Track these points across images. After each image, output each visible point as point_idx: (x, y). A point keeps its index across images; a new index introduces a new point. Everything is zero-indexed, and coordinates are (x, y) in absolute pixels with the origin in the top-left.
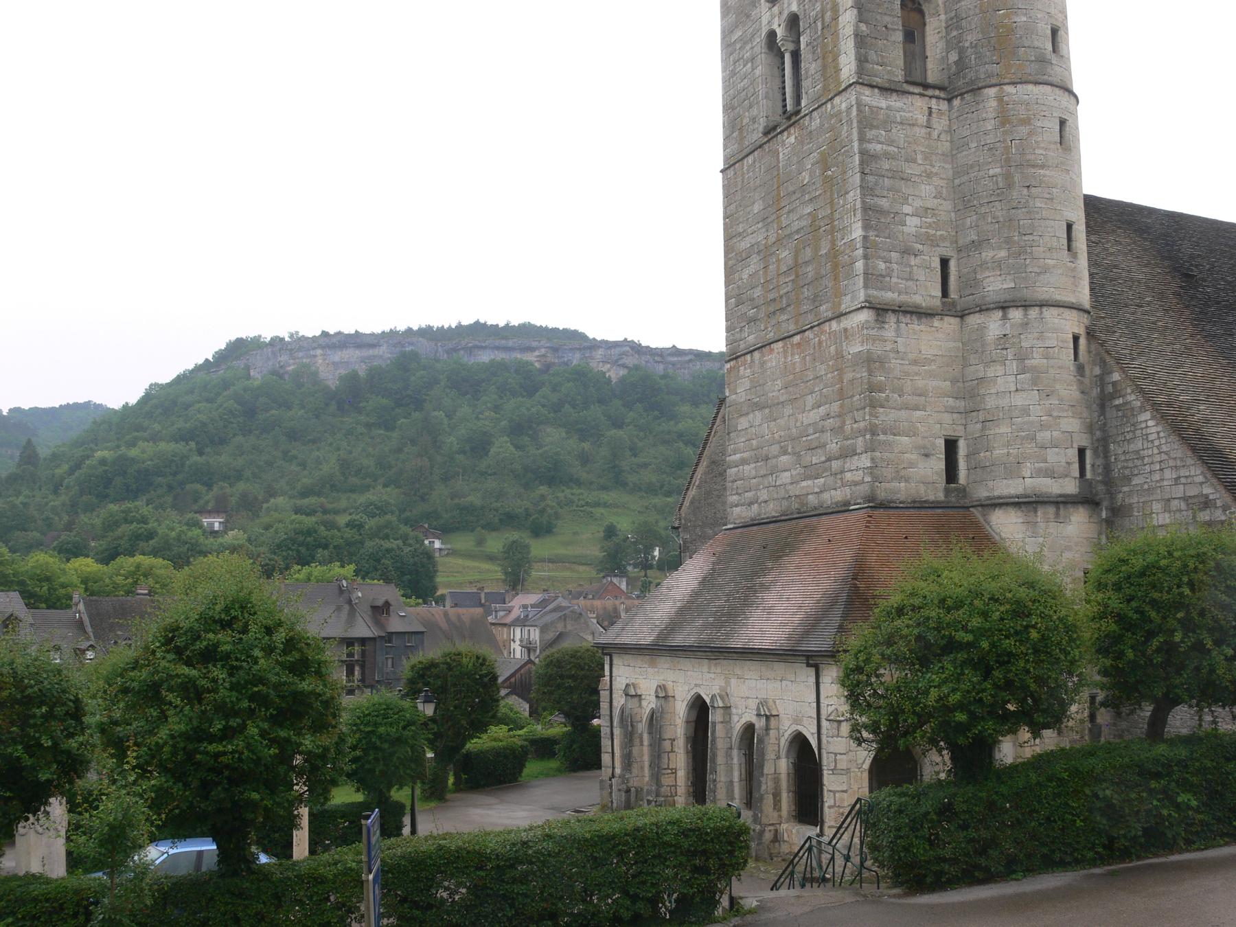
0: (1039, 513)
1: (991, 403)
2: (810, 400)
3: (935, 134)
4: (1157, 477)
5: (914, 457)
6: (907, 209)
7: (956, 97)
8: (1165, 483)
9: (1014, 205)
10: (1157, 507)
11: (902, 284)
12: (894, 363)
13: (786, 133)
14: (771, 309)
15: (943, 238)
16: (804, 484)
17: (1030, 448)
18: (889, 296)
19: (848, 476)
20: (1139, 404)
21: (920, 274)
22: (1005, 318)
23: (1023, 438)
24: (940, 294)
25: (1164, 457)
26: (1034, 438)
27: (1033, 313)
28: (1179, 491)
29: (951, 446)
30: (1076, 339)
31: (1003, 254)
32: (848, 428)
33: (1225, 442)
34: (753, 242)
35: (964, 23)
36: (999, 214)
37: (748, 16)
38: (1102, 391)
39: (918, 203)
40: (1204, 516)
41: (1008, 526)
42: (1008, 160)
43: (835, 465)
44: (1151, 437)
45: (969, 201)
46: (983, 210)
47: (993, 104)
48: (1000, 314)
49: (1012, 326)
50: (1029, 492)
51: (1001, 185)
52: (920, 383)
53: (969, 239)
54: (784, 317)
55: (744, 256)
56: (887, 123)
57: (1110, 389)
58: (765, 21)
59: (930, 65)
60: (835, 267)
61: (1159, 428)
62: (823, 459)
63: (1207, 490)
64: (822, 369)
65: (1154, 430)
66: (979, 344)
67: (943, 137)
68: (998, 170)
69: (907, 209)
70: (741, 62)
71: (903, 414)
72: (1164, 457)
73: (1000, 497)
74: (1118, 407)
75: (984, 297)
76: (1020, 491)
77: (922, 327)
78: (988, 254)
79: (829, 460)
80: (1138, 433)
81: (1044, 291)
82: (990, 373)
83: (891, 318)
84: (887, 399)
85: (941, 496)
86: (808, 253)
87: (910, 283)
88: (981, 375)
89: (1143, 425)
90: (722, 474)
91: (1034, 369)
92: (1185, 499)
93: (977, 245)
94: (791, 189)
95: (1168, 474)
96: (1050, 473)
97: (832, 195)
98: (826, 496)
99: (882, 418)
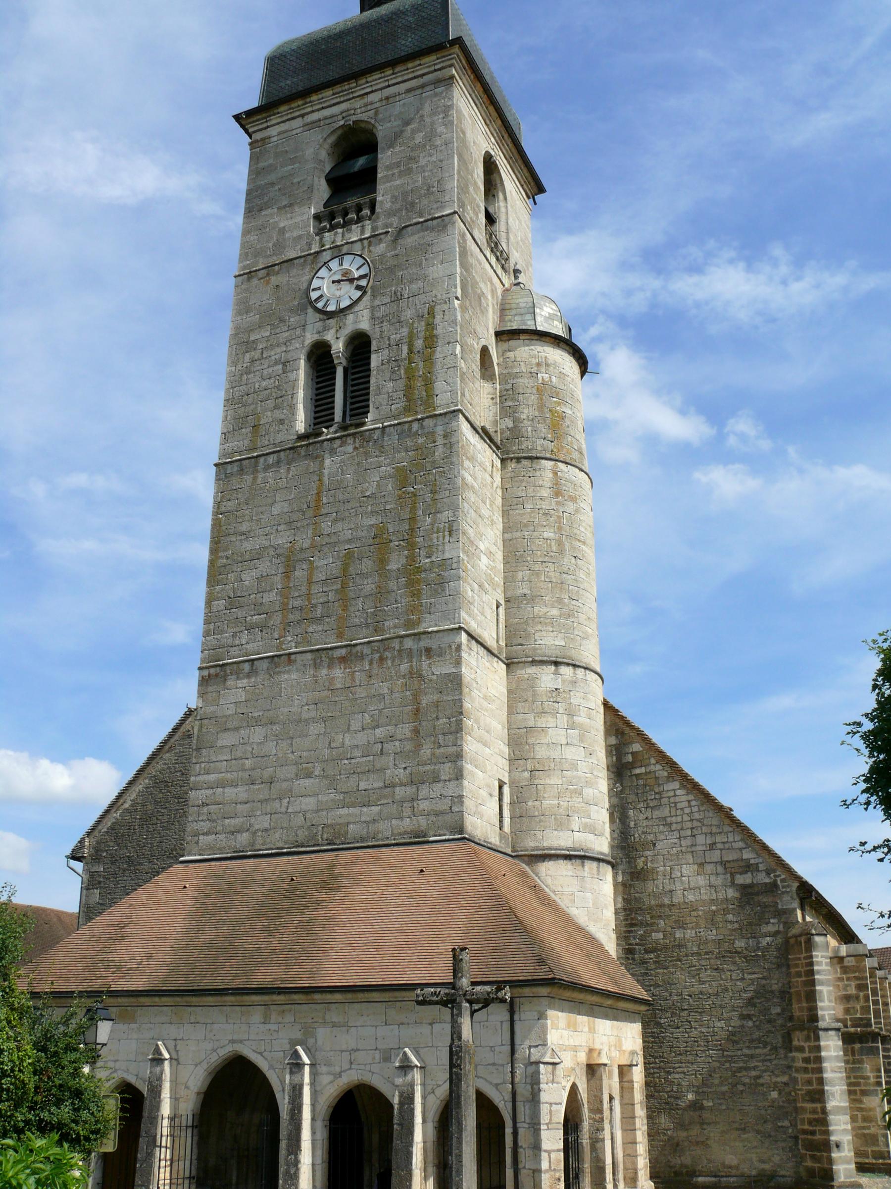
0: (586, 868)
1: (541, 752)
7: (511, 459)
8: (699, 848)
9: (565, 570)
13: (338, 442)
19: (424, 805)
20: (666, 774)
23: (572, 792)
25: (695, 824)
28: (716, 855)
31: (555, 612)
34: (267, 544)
35: (521, 397)
36: (552, 574)
38: (619, 759)
42: (560, 528)
44: (679, 806)
45: (521, 556)
46: (537, 567)
48: (553, 668)
49: (563, 681)
50: (577, 846)
51: (554, 549)
53: (520, 592)
54: (357, 620)
55: (247, 557)
57: (630, 758)
61: (691, 797)
62: (381, 784)
63: (747, 855)
65: (684, 798)
66: (530, 694)
68: (552, 535)
70: (266, 363)
72: (695, 824)
73: (550, 849)
74: (638, 776)
75: (535, 649)
76: (570, 844)
80: (665, 801)
82: (542, 722)
88: (531, 724)
89: (672, 794)
91: (580, 727)
92: (723, 863)
95: (701, 839)
97: (414, 509)
98: (382, 826)
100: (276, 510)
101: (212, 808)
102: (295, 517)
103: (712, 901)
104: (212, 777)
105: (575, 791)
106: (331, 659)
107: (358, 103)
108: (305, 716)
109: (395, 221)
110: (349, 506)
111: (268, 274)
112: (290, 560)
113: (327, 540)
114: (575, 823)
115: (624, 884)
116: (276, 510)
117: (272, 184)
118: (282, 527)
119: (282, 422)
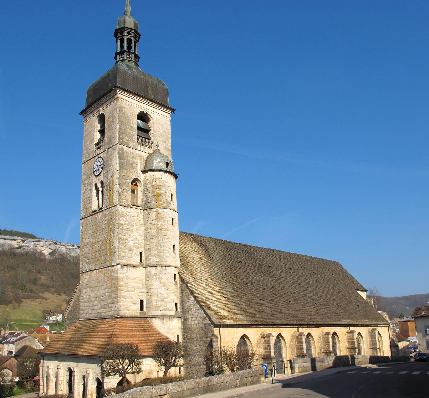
1: (152, 291)
2: (103, 287)
3: (139, 219)
4: (194, 312)
5: (131, 304)
6: (131, 239)
10: (194, 319)
11: (129, 259)
12: (126, 280)
15: (141, 247)
17: (162, 303)
18: (125, 262)
21: (134, 256)
22: (156, 269)
24: (139, 261)
26: (163, 300)
27: (164, 268)
28: (199, 315)
29: (142, 302)
30: (175, 275)
32: (113, 296)
33: (211, 303)
37: (90, 178)
39: (134, 237)
40: (204, 322)
41: (156, 323)
43: (110, 305)
46: (151, 240)
47: (155, 213)
52: (133, 285)
56: (126, 215)
58: (94, 181)
59: (139, 200)
60: (110, 252)
64: (106, 279)
67: (141, 220)
69: (131, 239)
71: (128, 293)
76: (160, 314)
77: (134, 270)
78: (152, 252)
79: (108, 304)
81: (166, 263)
83: (125, 267)
84: (124, 289)
85: (139, 315)
86: (103, 247)
87: (131, 258)
91: (163, 283)
92: (201, 317)
93: (150, 249)
94: (99, 229)
95: (197, 311)
96: (167, 310)
99: (122, 294)
103: (199, 328)
105: (161, 300)
114: (161, 308)
115: (183, 322)
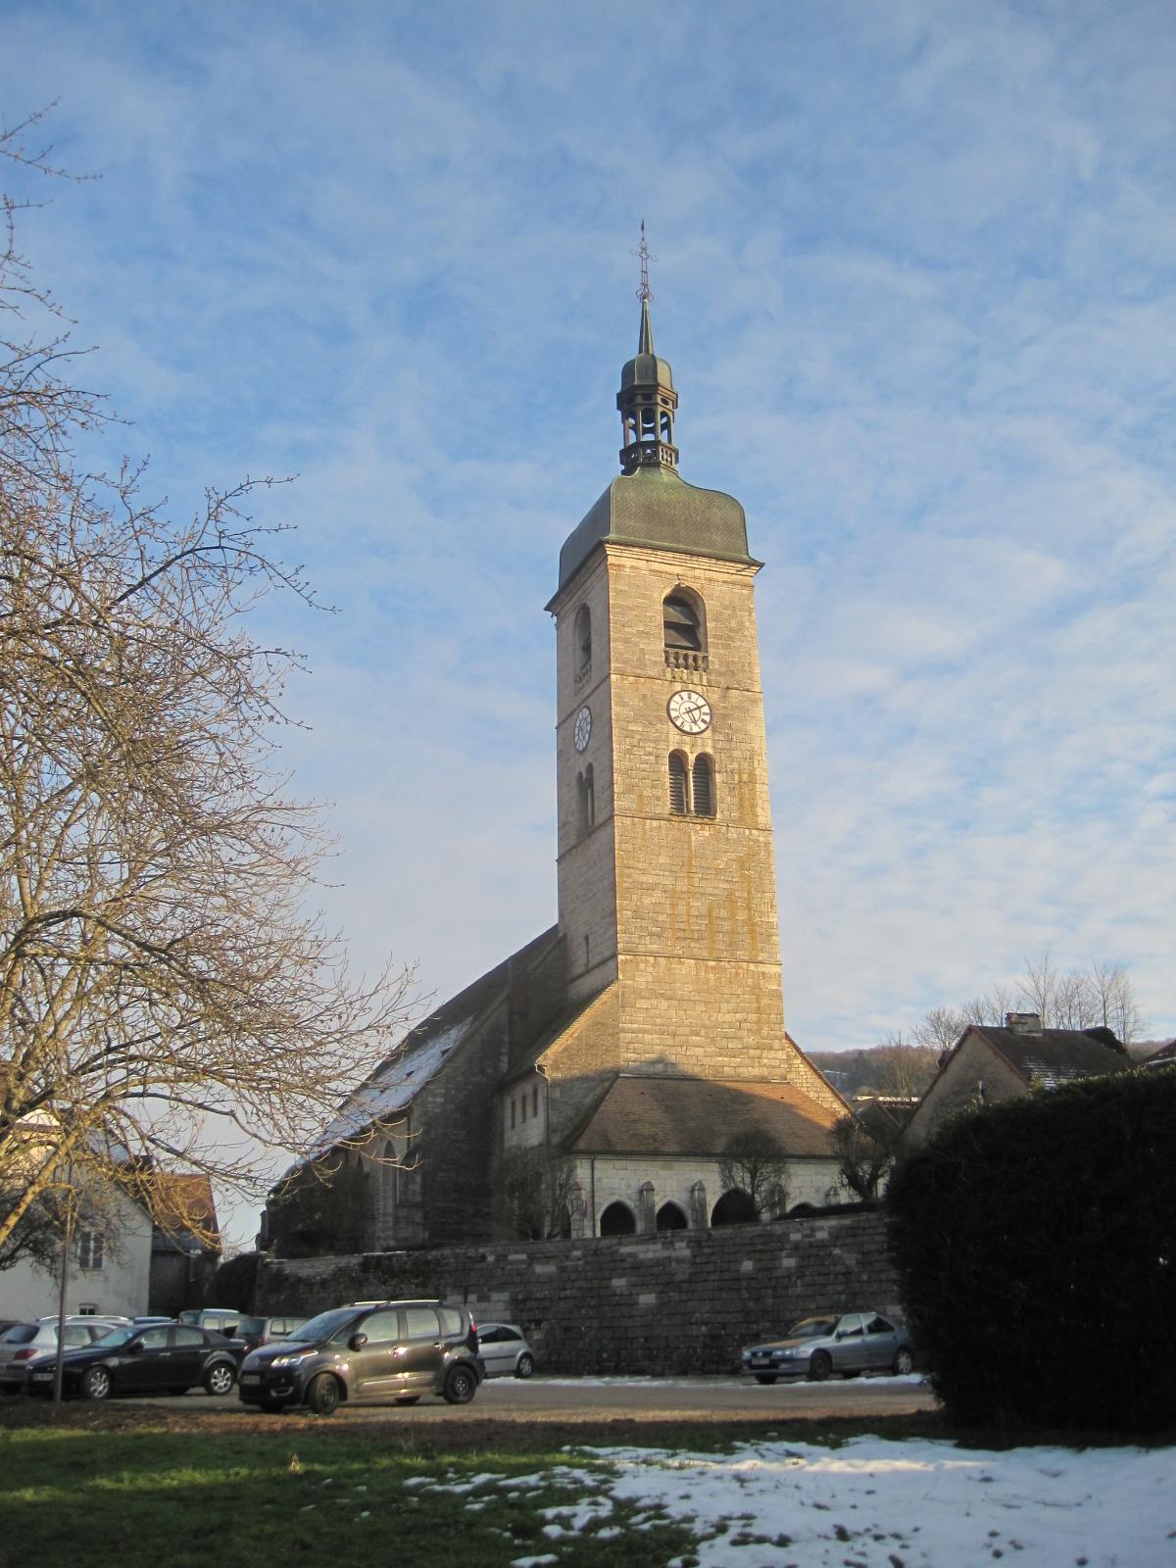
13: (698, 827)
14: (681, 934)
16: (720, 1059)
55: (644, 886)
90: (614, 1035)
100: (662, 860)
101: (636, 1045)
102: (674, 868)
104: (636, 1026)
106: (707, 966)
107: (689, 573)
108: (693, 998)
109: (722, 680)
110: (711, 871)
111: (636, 682)
112: (674, 896)
113: (697, 890)
116: (662, 860)
117: (630, 608)
118: (666, 873)
119: (658, 798)
